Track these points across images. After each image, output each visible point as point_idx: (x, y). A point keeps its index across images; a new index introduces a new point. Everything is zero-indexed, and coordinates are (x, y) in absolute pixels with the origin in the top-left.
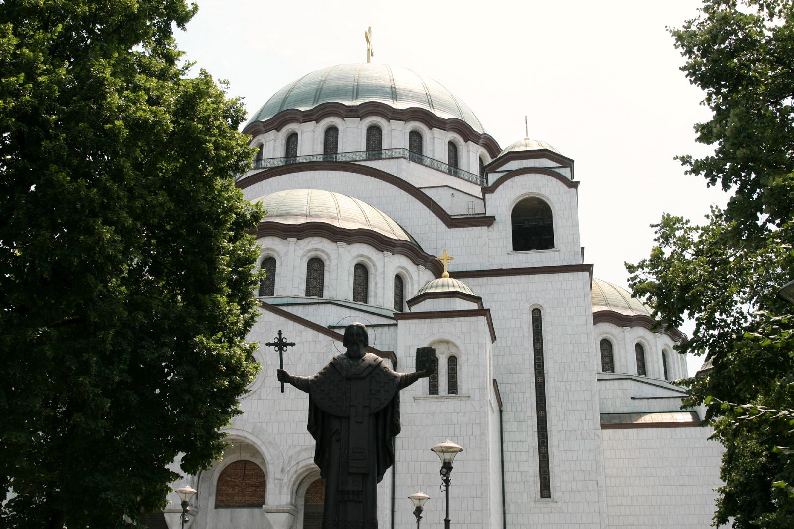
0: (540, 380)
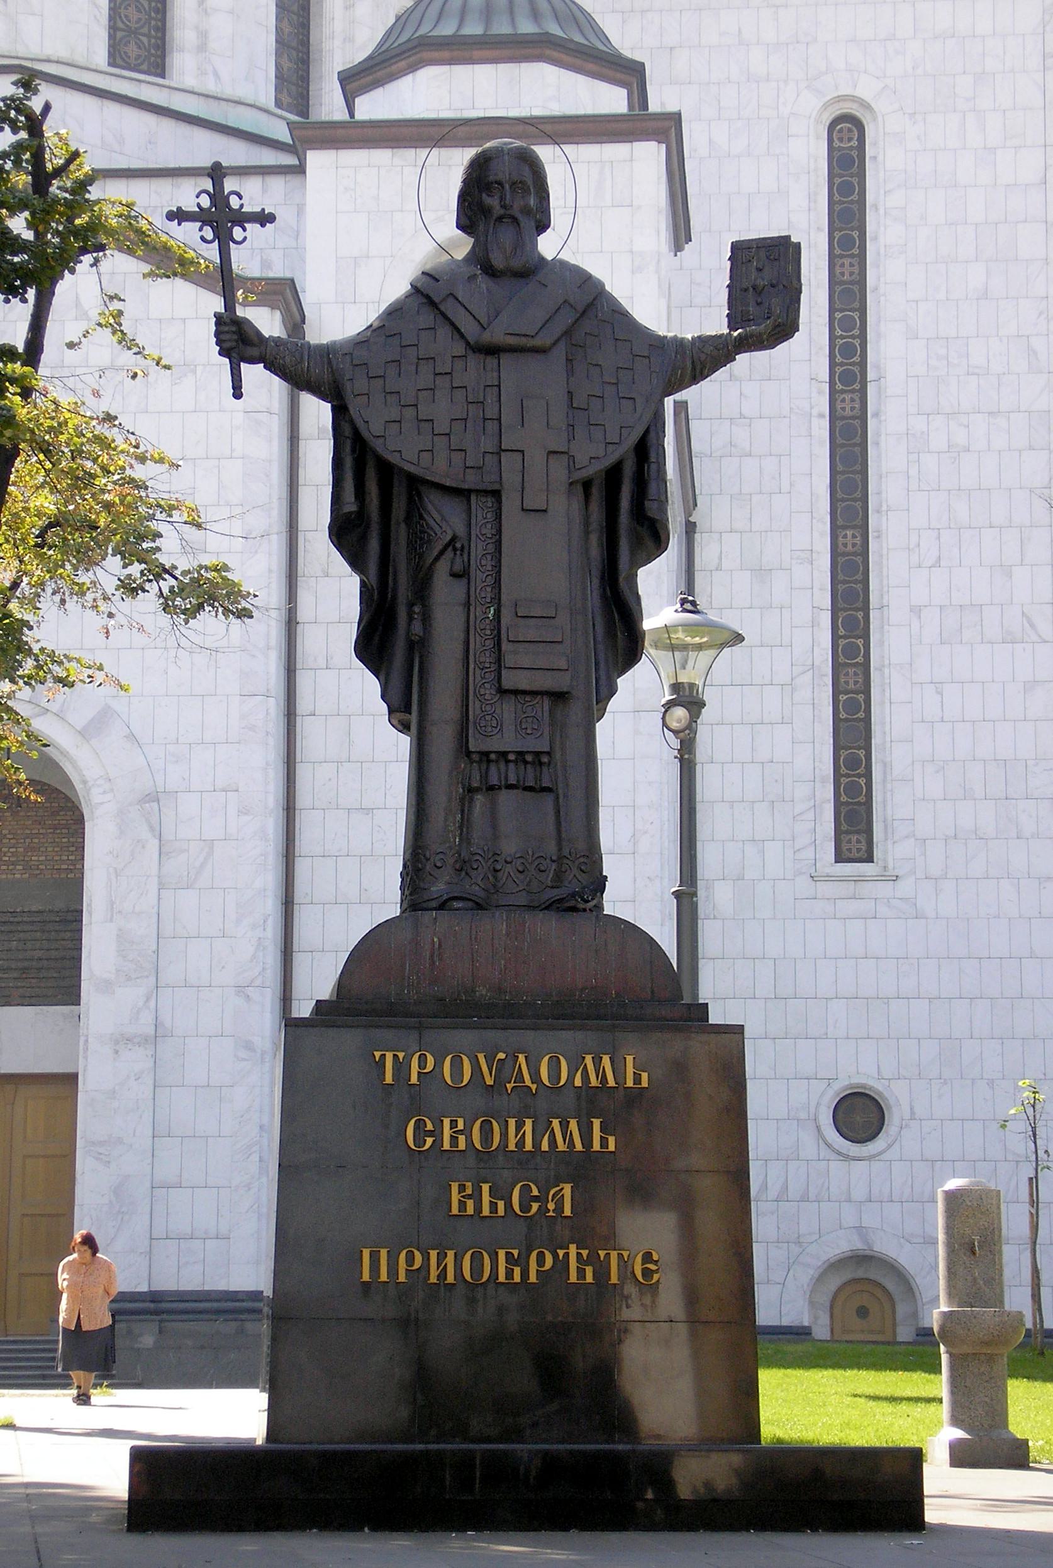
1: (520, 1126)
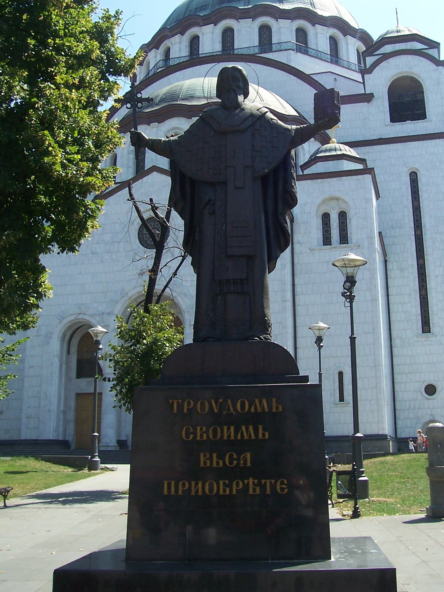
0: (418, 233)
1: (229, 429)
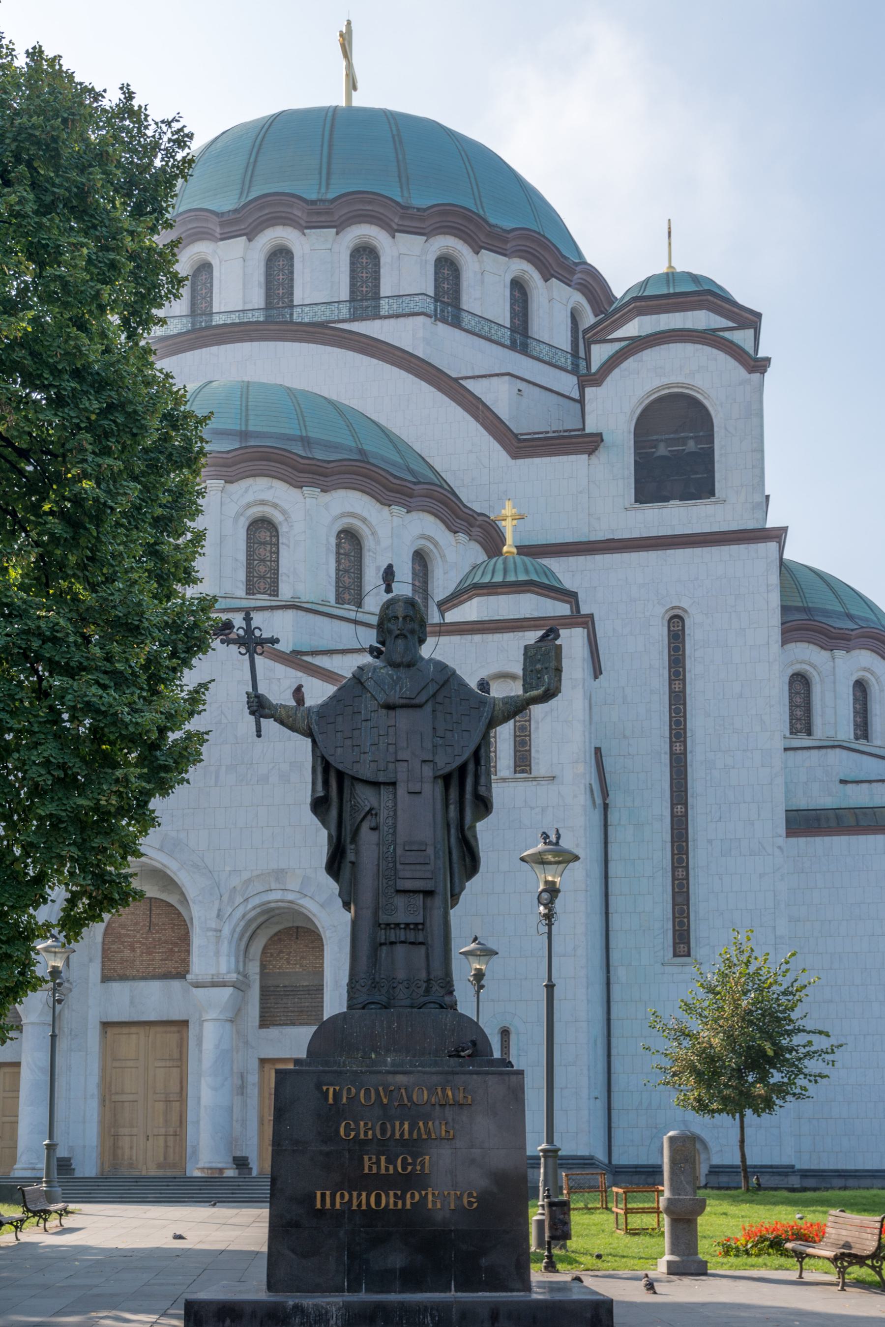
1: (402, 1124)
